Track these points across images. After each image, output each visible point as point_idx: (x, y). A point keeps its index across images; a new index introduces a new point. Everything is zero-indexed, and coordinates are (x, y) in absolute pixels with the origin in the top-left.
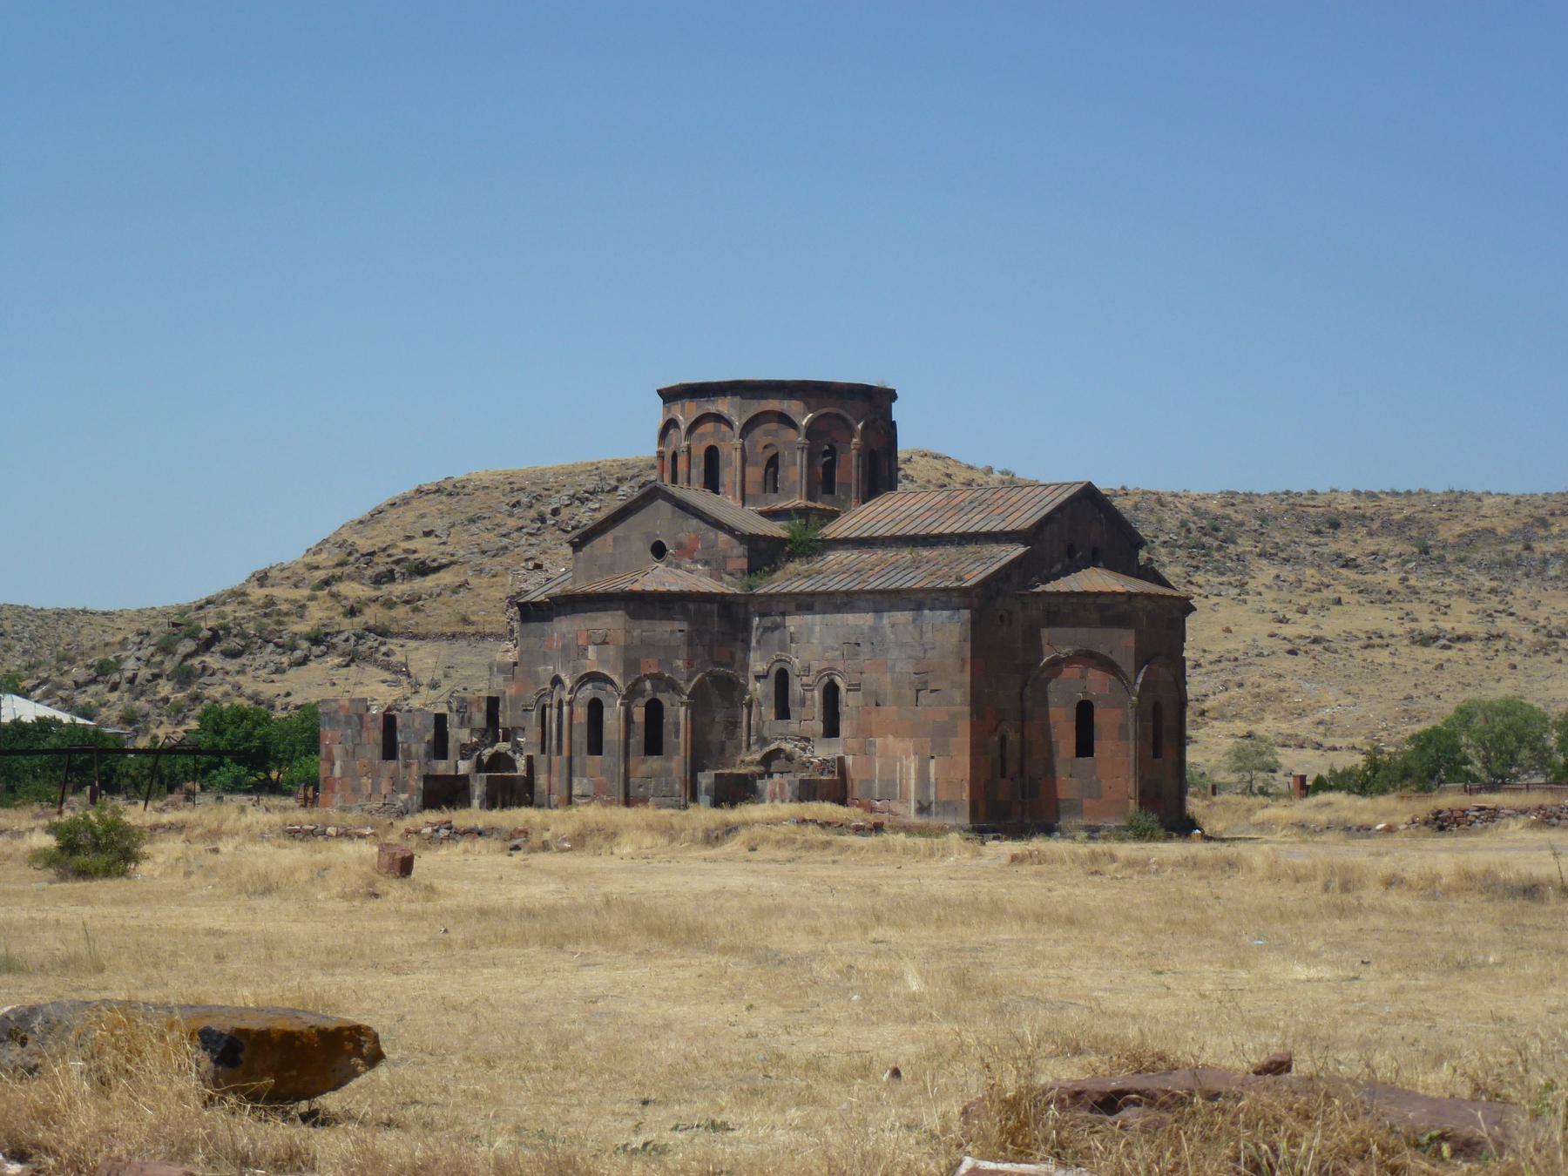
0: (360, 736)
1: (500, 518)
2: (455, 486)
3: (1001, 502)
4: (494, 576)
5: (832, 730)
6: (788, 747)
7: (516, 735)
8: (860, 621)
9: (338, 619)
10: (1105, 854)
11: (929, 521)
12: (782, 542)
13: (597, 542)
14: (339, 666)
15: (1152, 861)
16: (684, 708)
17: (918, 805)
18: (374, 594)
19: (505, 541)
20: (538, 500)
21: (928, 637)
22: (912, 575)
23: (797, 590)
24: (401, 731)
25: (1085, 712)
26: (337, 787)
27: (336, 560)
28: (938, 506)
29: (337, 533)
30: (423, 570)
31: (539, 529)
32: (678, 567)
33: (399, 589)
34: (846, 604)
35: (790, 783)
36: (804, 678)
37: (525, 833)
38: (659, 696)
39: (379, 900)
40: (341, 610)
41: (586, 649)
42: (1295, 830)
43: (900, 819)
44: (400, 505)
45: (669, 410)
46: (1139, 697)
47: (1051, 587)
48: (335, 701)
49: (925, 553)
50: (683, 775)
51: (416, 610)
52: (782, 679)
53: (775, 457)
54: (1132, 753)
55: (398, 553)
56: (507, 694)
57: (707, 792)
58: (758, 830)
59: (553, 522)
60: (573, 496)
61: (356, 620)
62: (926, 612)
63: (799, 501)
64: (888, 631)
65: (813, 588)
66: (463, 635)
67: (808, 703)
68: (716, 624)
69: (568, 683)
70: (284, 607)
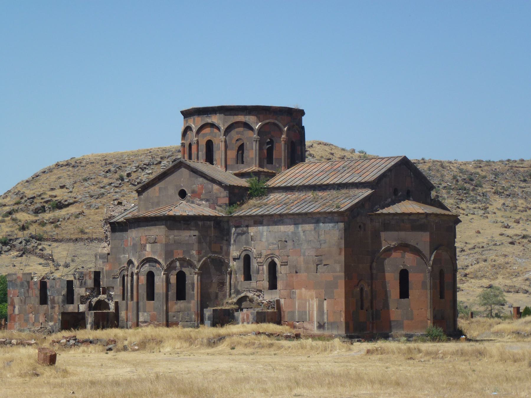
1: (100, 179)
2: (76, 162)
3: (359, 167)
4: (97, 209)
5: (273, 286)
6: (250, 295)
7: (109, 291)
8: (287, 229)
9: (16, 232)
10: (415, 349)
11: (322, 177)
12: (246, 189)
13: (150, 191)
14: (17, 256)
15: (440, 352)
16: (196, 276)
17: (318, 325)
18: (34, 218)
19: (103, 190)
20: (119, 169)
21: (322, 237)
22: (313, 205)
23: (254, 214)
24: (49, 290)
25: (404, 275)
26: (17, 319)
27: (14, 201)
28: (327, 170)
29: (15, 187)
30: (60, 206)
31: (120, 184)
32: (193, 202)
33: (47, 216)
34: (280, 221)
35: (252, 314)
36: (258, 259)
37: (114, 342)
38: (184, 270)
39: (38, 377)
40: (17, 227)
41: (145, 246)
42: (514, 335)
43: (309, 332)
44: (47, 172)
45: (186, 122)
46: (432, 267)
47: (385, 211)
48: (15, 274)
49: (320, 194)
50: (196, 310)
51: (56, 227)
52: (247, 260)
53: (242, 145)
54: (429, 296)
55: (47, 197)
56: (104, 270)
57: (209, 319)
58: (235, 339)
59: (127, 180)
60: (138, 167)
61: (25, 232)
62: (321, 224)
63: (255, 168)
64: (302, 234)
65: (262, 213)
66: (82, 239)
67: (260, 272)
68: (213, 232)
69: (136, 263)
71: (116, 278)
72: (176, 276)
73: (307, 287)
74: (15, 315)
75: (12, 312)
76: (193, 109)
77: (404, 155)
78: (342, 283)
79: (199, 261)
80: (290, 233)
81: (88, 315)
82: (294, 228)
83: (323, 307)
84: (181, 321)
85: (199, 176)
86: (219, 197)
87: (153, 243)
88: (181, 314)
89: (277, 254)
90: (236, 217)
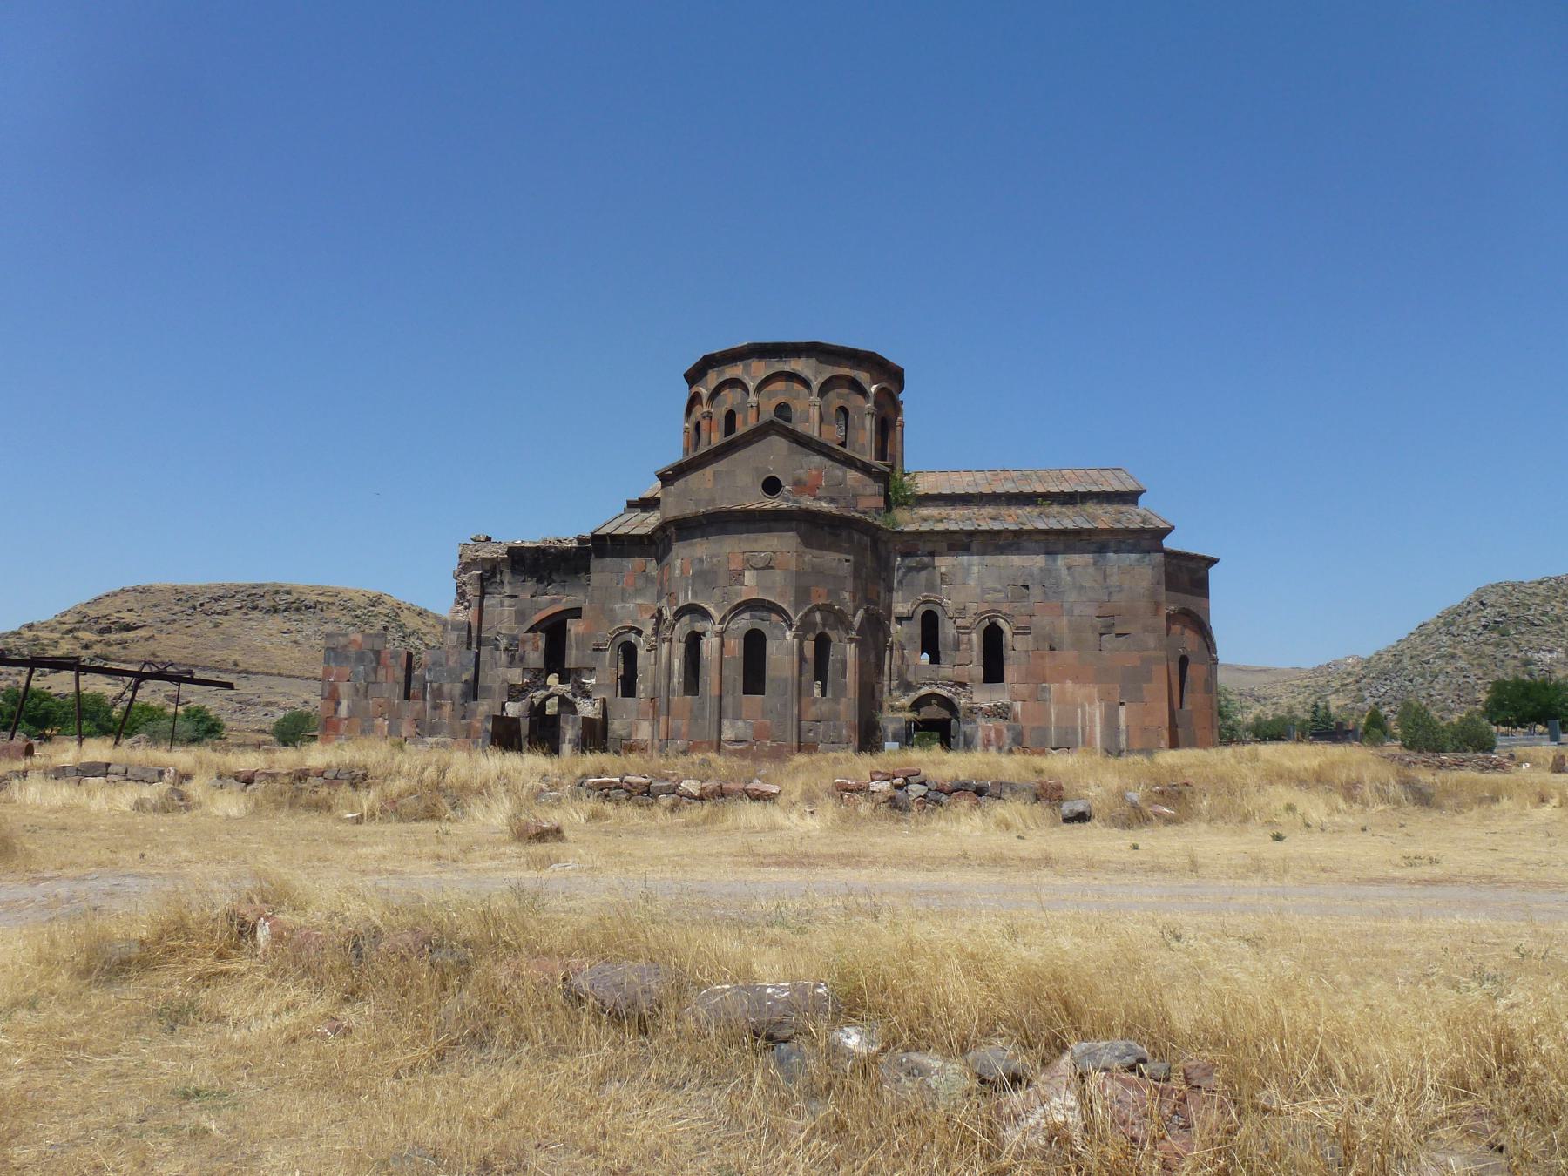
0: (376, 673)
5: (993, 672)
7: (580, 676)
16: (853, 645)
19: (174, 617)
21: (1114, 580)
26: (342, 728)
27: (76, 620)
29: (76, 607)
30: (128, 628)
33: (113, 637)
34: (1011, 545)
38: (827, 631)
51: (124, 648)
52: (930, 623)
57: (895, 738)
62: (1111, 555)
64: (1064, 572)
67: (963, 647)
70: (46, 642)
71: (601, 650)
74: (340, 720)
75: (331, 713)
76: (749, 345)
80: (1035, 570)
83: (1118, 720)
88: (822, 726)
89: (1006, 610)
90: (909, 533)
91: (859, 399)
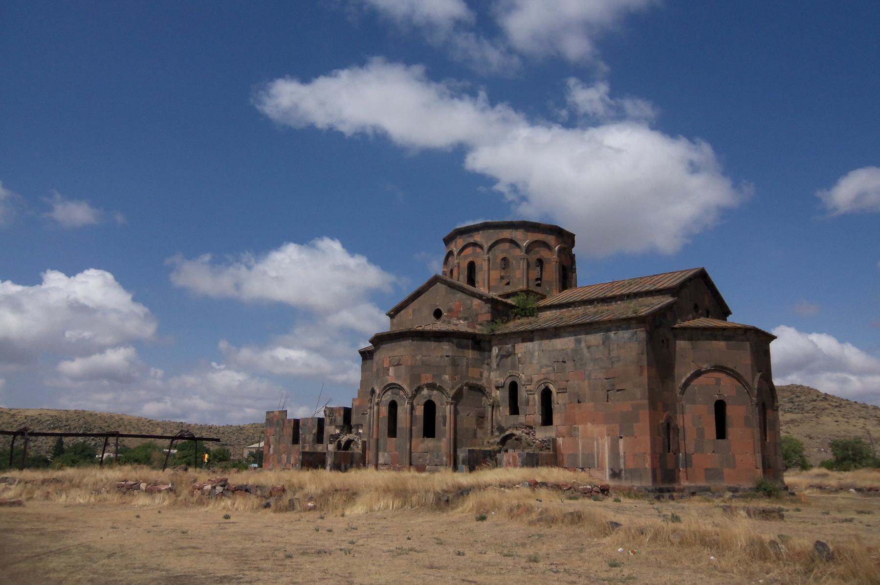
0: (283, 431)
6: (518, 433)
8: (565, 343)
16: (449, 406)
17: (611, 472)
21: (614, 353)
36: (528, 386)
41: (388, 369)
52: (514, 388)
58: (489, 496)
64: (585, 351)
72: (423, 406)
73: (594, 420)
75: (267, 453)
77: (702, 267)
78: (644, 415)
79: (453, 388)
80: (569, 351)
81: (328, 455)
82: (575, 344)
84: (428, 465)
85: (456, 291)
86: (479, 314)
87: (396, 365)
89: (553, 378)
90: (499, 335)
91: (517, 252)
